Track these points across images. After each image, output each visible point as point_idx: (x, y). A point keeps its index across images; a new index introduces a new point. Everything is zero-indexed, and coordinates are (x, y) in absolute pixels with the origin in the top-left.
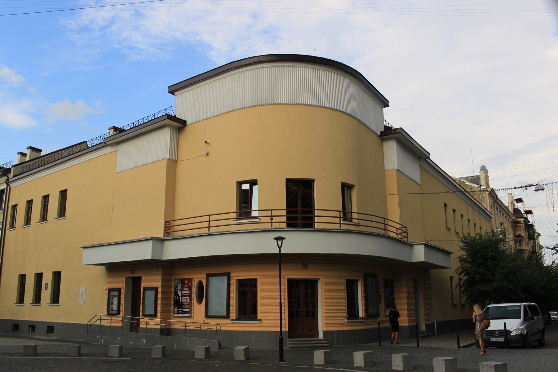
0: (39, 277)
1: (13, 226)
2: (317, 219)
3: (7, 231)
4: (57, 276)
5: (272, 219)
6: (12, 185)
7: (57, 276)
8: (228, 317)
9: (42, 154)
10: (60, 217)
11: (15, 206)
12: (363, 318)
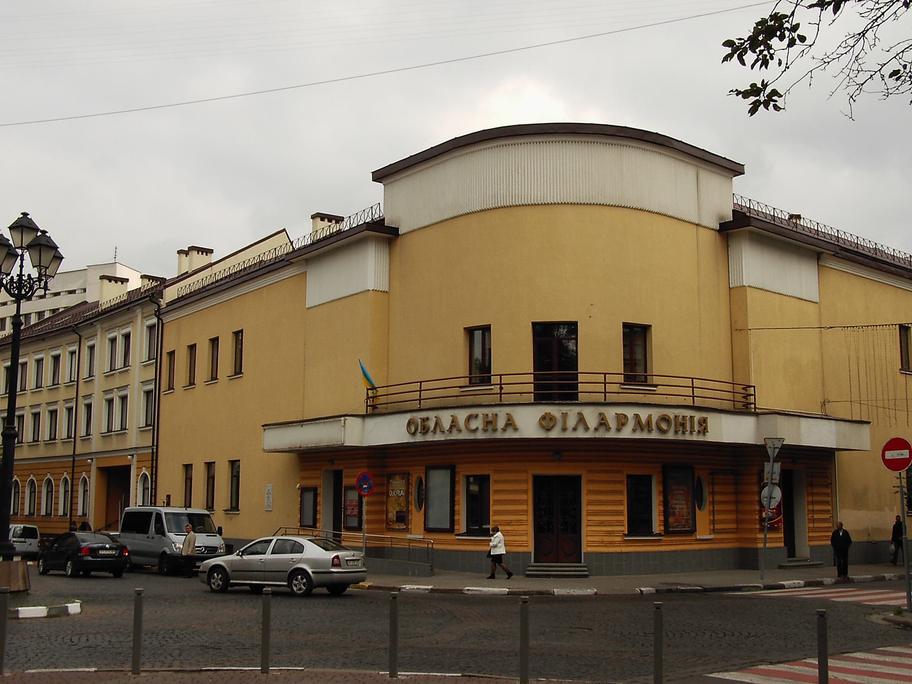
0: (210, 466)
1: (171, 387)
2: (581, 387)
3: (162, 394)
4: (234, 464)
5: (501, 388)
6: (166, 319)
7: (234, 464)
8: (451, 530)
9: (214, 258)
10: (236, 374)
11: (172, 354)
12: (659, 535)
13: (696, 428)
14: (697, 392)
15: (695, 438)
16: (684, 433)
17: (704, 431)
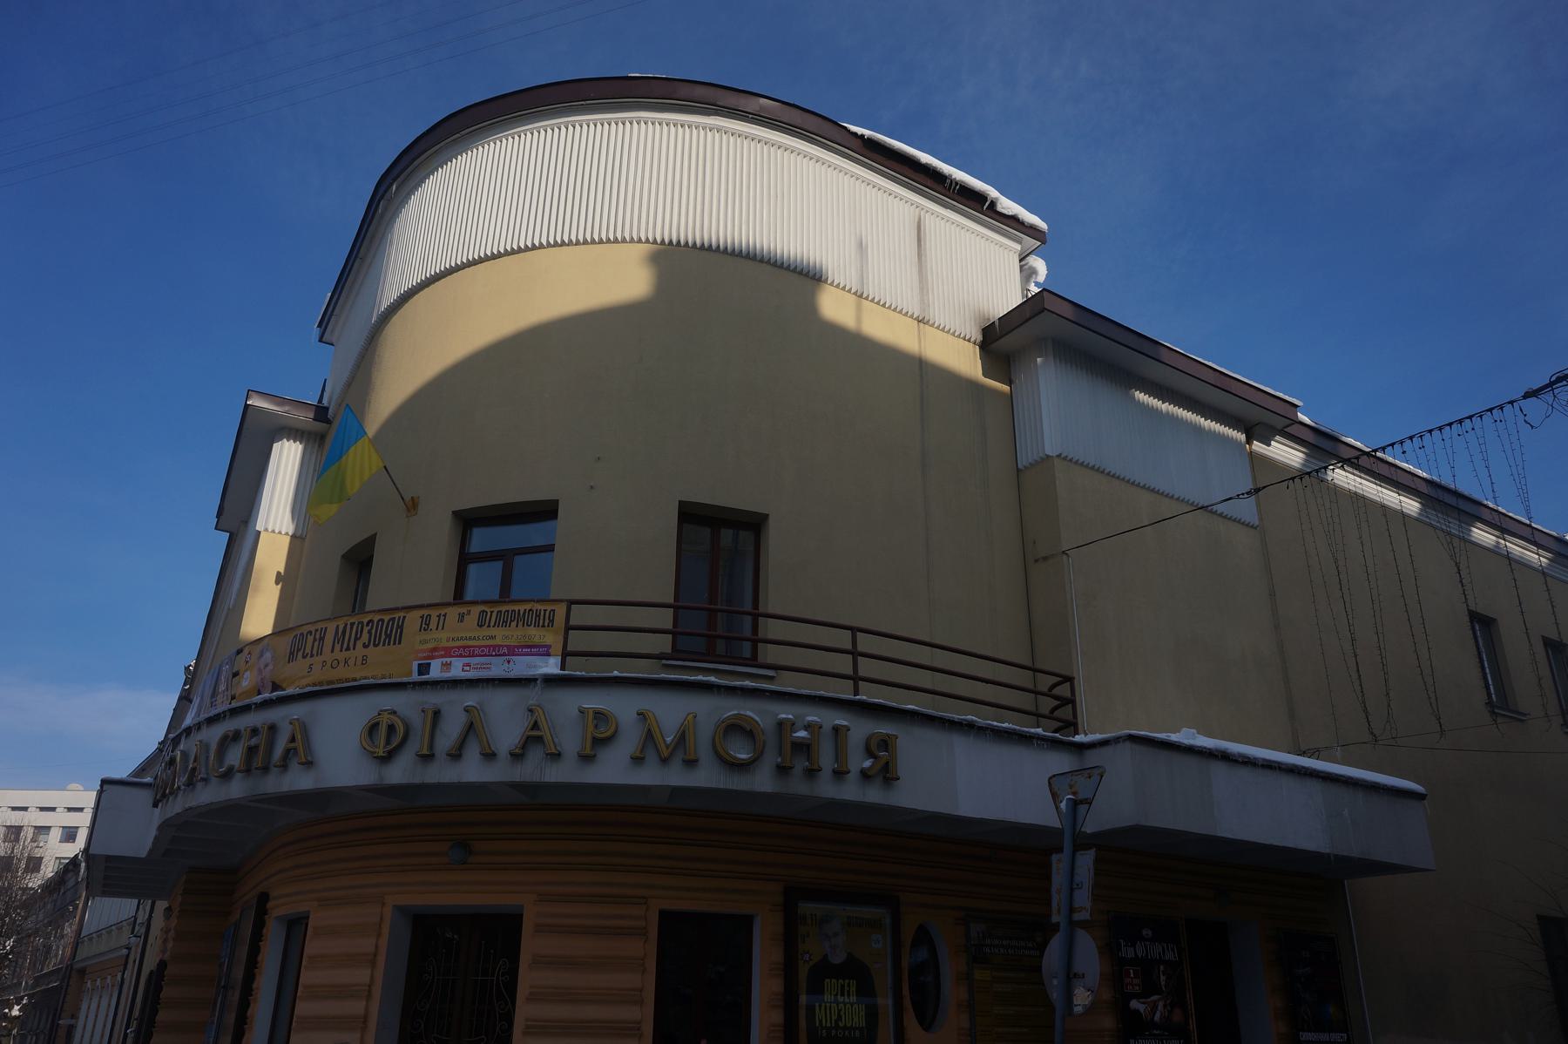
13: (859, 762)
14: (867, 667)
15: (851, 791)
16: (812, 773)
17: (886, 774)
